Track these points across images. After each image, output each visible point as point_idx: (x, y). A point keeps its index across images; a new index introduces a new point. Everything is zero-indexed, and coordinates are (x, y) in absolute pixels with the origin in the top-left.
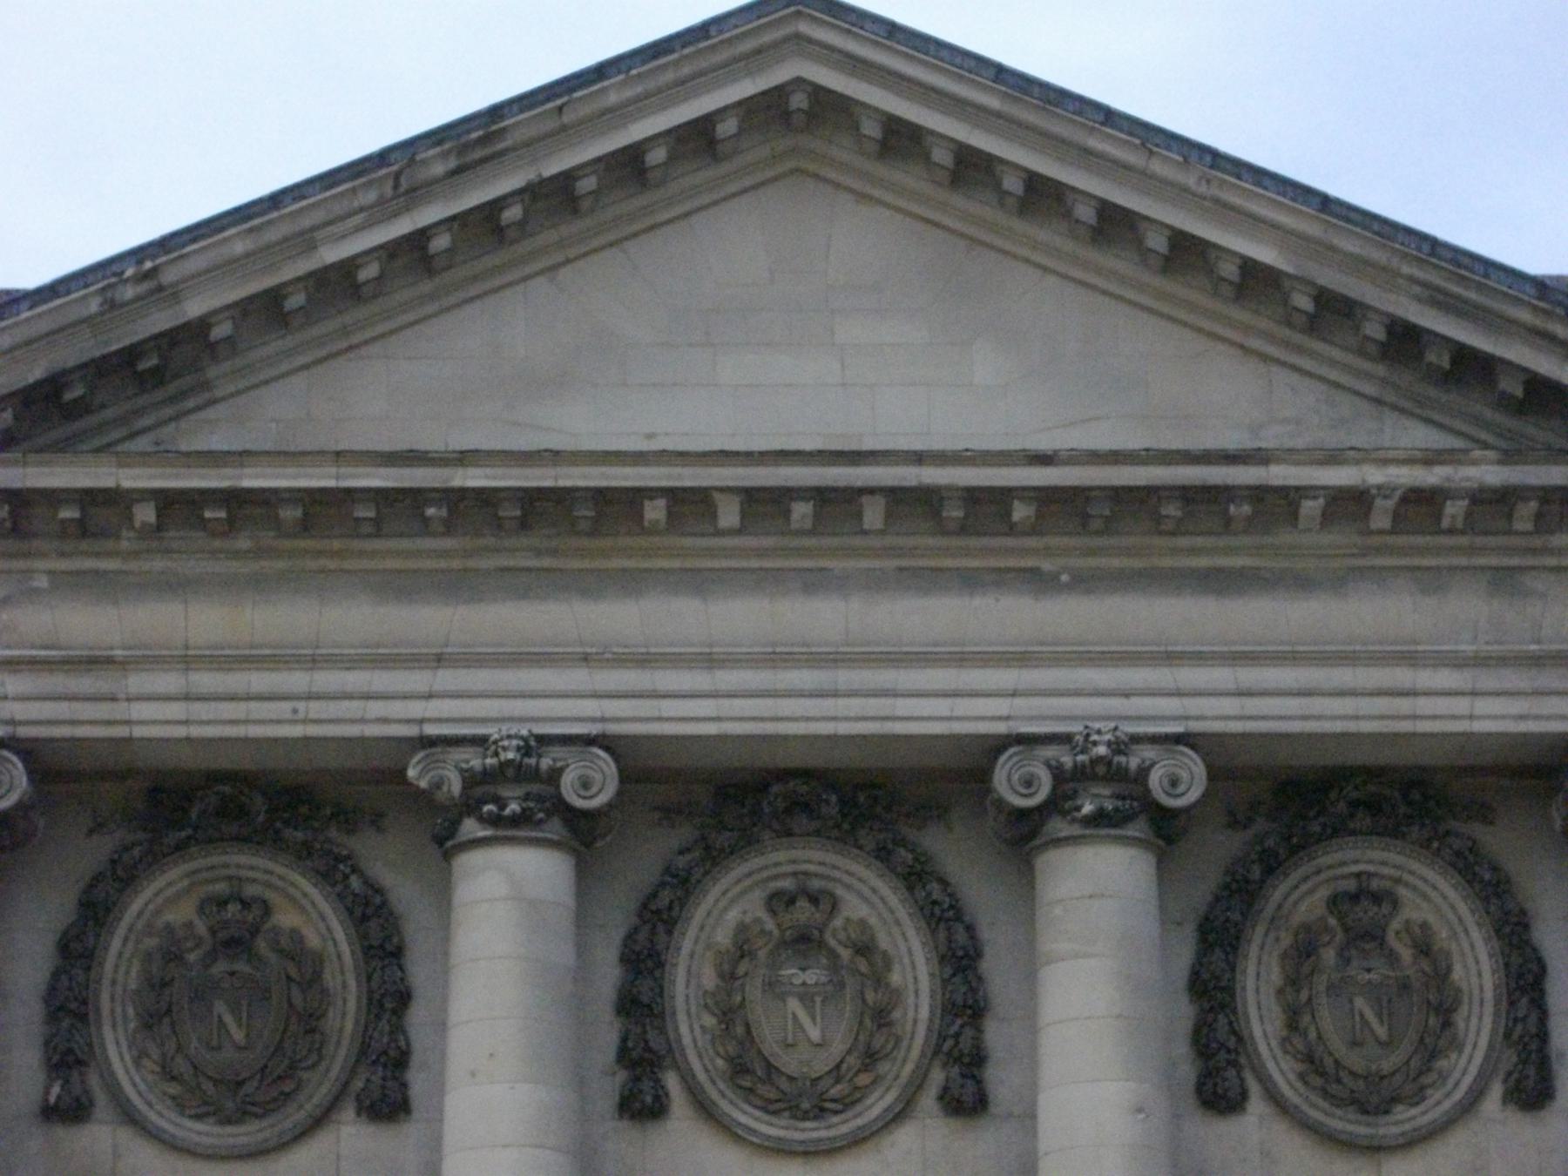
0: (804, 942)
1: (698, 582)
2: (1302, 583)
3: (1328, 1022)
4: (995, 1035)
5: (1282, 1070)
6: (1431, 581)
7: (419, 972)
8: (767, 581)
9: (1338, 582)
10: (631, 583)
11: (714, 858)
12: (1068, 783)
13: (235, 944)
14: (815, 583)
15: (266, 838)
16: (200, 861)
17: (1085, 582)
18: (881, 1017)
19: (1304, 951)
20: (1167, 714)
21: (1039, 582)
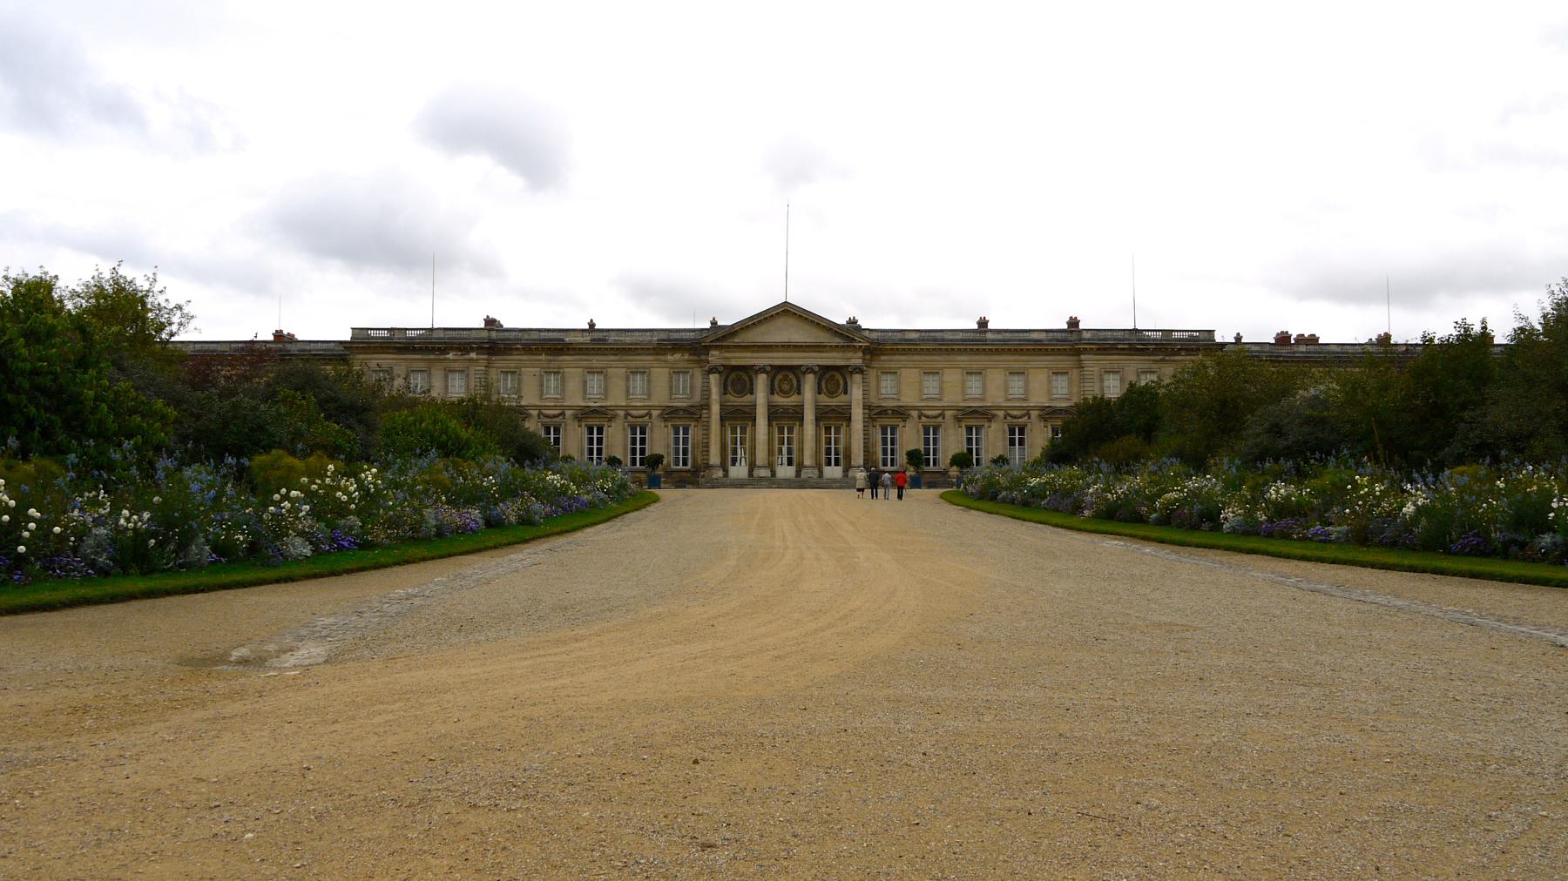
0: (786, 380)
1: (778, 352)
2: (827, 352)
3: (829, 386)
4: (802, 388)
5: (825, 391)
6: (837, 352)
7: (754, 382)
8: (782, 351)
9: (830, 352)
10: (773, 352)
11: (779, 373)
12: (807, 369)
13: (739, 379)
14: (787, 352)
15: (741, 371)
16: (736, 373)
17: (809, 352)
18: (792, 385)
19: (827, 381)
20: (816, 363)
21: (804, 351)
